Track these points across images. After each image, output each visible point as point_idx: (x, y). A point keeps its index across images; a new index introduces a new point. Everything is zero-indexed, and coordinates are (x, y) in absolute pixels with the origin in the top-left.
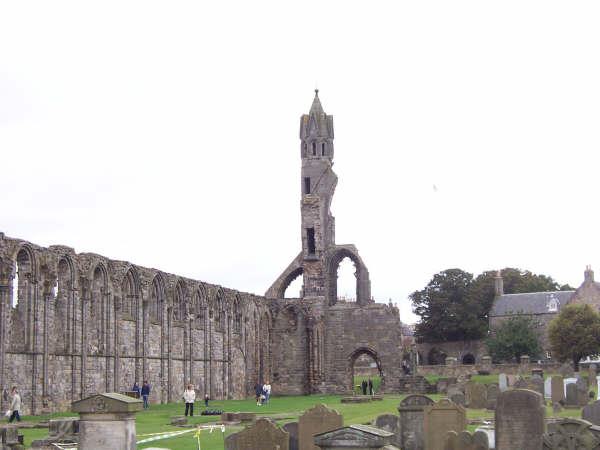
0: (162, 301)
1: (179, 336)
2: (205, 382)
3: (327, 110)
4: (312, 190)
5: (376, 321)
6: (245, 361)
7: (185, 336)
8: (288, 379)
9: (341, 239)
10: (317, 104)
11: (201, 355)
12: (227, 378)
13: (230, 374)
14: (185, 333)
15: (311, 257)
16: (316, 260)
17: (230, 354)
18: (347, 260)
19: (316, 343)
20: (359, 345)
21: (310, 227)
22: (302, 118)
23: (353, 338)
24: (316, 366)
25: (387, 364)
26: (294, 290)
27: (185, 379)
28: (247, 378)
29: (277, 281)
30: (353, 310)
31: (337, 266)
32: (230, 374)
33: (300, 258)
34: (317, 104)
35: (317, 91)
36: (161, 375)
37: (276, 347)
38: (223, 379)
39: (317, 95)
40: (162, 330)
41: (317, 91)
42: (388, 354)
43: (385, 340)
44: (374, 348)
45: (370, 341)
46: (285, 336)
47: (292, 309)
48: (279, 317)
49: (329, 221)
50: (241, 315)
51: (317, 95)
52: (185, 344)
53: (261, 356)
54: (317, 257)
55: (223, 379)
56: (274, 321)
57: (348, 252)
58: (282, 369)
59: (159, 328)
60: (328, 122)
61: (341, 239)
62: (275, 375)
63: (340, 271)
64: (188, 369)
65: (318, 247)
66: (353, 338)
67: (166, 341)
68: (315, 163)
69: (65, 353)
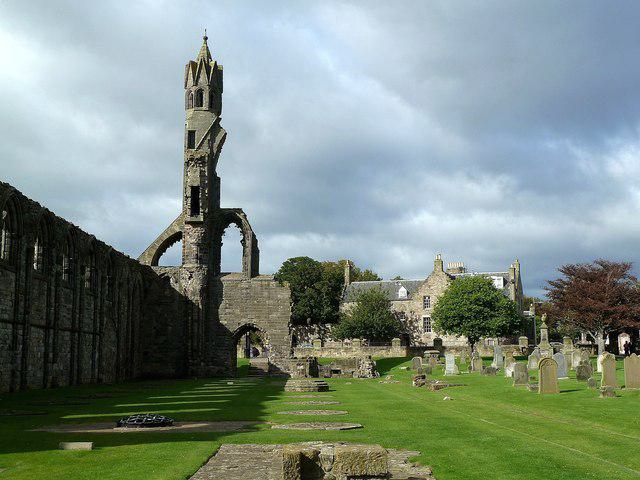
0: (19, 237)
1: (41, 294)
2: (72, 360)
3: (217, 58)
6: (117, 336)
7: (49, 295)
9: (225, 204)
11: (68, 324)
13: (100, 350)
14: (49, 289)
17: (102, 324)
18: (232, 225)
19: (196, 318)
23: (238, 311)
27: (46, 355)
28: (118, 355)
32: (100, 350)
35: (206, 38)
36: (13, 347)
38: (93, 355)
40: (17, 280)
49: (214, 183)
52: (49, 305)
53: (133, 331)
55: (93, 355)
57: (234, 216)
59: (12, 277)
61: (225, 204)
63: (224, 240)
64: (51, 341)
66: (238, 311)
67: (21, 297)
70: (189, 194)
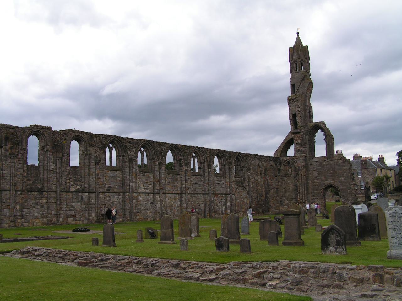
4: (296, 91)
5: (337, 167)
8: (288, 203)
9: (316, 119)
10: (298, 41)
12: (228, 204)
15: (296, 131)
16: (299, 133)
18: (320, 131)
20: (327, 182)
21: (294, 113)
22: (290, 48)
24: (301, 196)
25: (344, 194)
26: (291, 152)
29: (280, 147)
30: (323, 161)
31: (315, 136)
33: (291, 133)
34: (298, 41)
35: (298, 33)
37: (281, 185)
39: (298, 36)
41: (298, 33)
42: (345, 187)
43: (342, 178)
44: (336, 184)
45: (334, 180)
46: (285, 179)
47: (290, 162)
48: (282, 168)
49: (309, 111)
50: (244, 167)
51: (298, 36)
52: (182, 184)
54: (299, 131)
55: (225, 204)
56: (279, 170)
57: (321, 126)
58: (285, 198)
60: (306, 49)
61: (316, 119)
62: (281, 201)
63: (316, 139)
65: (300, 124)
66: (323, 178)
68: (297, 75)
69: (41, 191)
70: (291, 119)
